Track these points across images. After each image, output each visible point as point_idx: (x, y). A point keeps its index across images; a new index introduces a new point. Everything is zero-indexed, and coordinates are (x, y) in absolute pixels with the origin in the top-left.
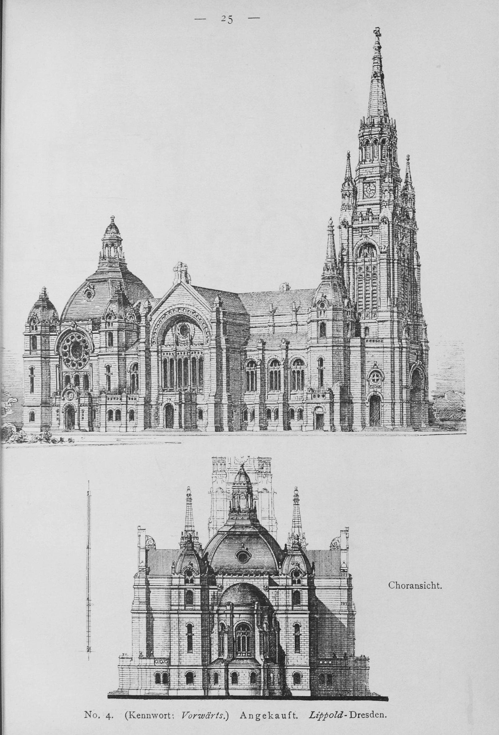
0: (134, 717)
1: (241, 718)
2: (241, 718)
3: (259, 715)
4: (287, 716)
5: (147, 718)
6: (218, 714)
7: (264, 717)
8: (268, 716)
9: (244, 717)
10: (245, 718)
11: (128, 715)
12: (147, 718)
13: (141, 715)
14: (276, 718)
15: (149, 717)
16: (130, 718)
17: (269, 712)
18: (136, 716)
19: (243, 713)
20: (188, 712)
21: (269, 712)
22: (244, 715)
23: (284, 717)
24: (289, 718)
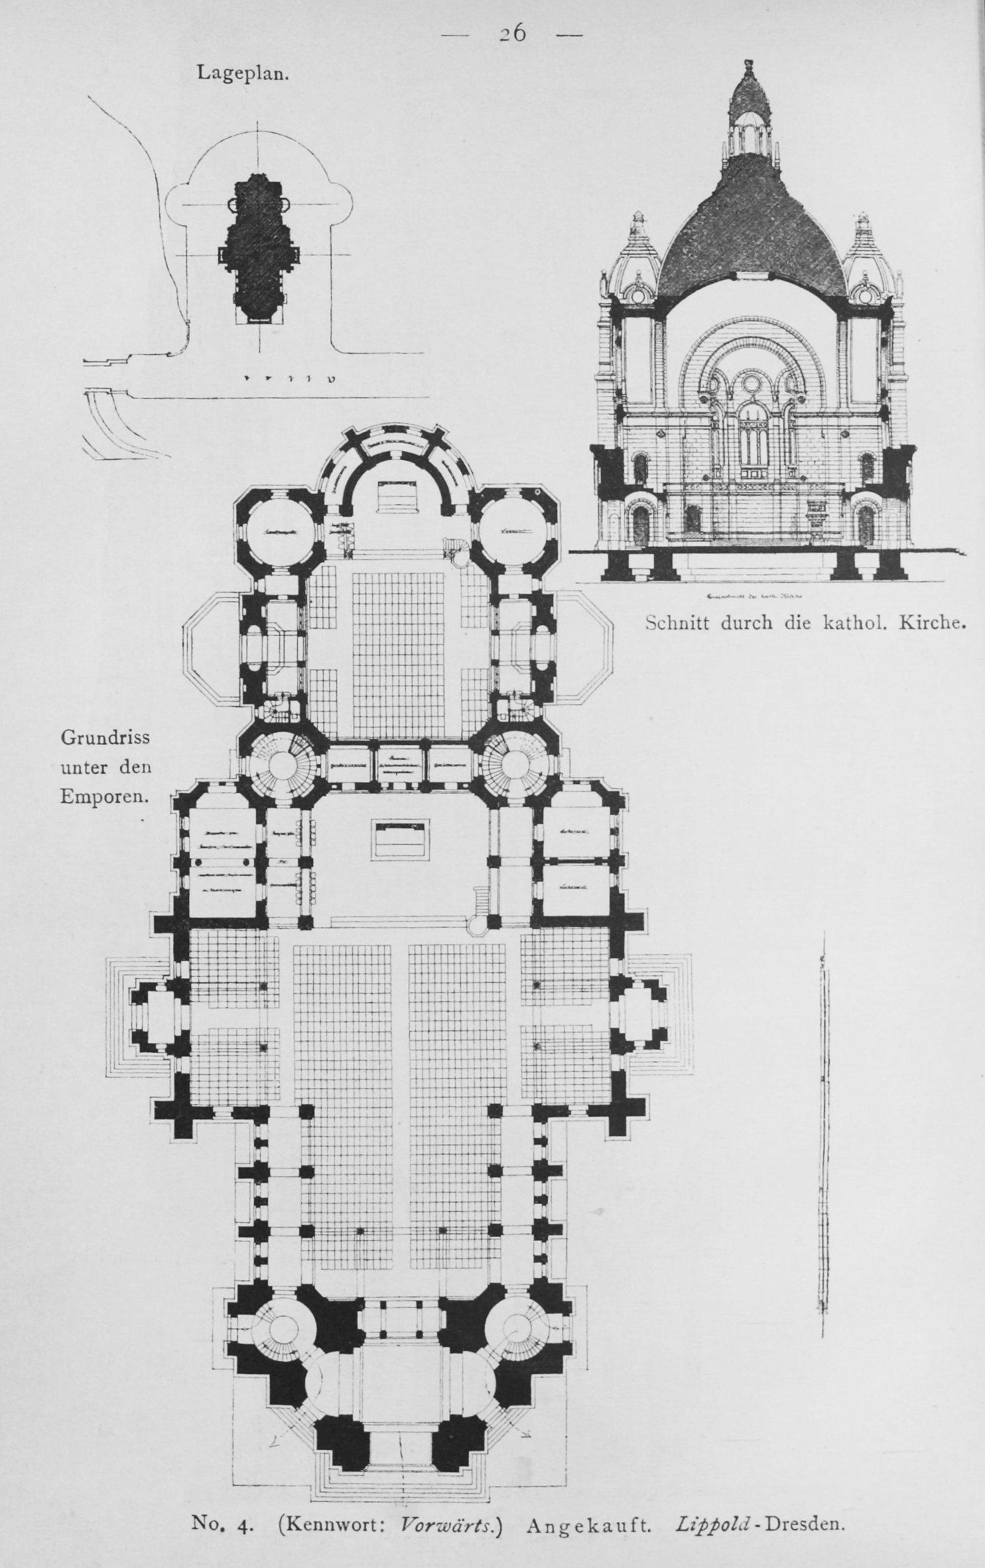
0: (298, 1529)
1: (529, 1532)
2: (529, 1532)
3: (567, 1525)
4: (629, 1527)
5: (327, 1529)
6: (480, 1523)
7: (580, 1529)
8: (586, 1528)
9: (535, 1530)
10: (538, 1531)
11: (285, 1521)
12: (327, 1529)
13: (313, 1524)
14: (605, 1531)
15: (330, 1528)
16: (290, 1529)
17: (590, 1519)
18: (301, 1526)
19: (534, 1521)
20: (415, 1518)
21: (590, 1519)
22: (536, 1527)
23: (621, 1529)
24: (633, 1531)
